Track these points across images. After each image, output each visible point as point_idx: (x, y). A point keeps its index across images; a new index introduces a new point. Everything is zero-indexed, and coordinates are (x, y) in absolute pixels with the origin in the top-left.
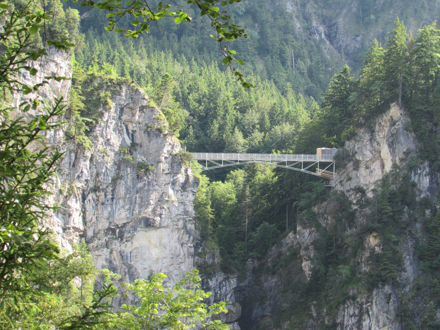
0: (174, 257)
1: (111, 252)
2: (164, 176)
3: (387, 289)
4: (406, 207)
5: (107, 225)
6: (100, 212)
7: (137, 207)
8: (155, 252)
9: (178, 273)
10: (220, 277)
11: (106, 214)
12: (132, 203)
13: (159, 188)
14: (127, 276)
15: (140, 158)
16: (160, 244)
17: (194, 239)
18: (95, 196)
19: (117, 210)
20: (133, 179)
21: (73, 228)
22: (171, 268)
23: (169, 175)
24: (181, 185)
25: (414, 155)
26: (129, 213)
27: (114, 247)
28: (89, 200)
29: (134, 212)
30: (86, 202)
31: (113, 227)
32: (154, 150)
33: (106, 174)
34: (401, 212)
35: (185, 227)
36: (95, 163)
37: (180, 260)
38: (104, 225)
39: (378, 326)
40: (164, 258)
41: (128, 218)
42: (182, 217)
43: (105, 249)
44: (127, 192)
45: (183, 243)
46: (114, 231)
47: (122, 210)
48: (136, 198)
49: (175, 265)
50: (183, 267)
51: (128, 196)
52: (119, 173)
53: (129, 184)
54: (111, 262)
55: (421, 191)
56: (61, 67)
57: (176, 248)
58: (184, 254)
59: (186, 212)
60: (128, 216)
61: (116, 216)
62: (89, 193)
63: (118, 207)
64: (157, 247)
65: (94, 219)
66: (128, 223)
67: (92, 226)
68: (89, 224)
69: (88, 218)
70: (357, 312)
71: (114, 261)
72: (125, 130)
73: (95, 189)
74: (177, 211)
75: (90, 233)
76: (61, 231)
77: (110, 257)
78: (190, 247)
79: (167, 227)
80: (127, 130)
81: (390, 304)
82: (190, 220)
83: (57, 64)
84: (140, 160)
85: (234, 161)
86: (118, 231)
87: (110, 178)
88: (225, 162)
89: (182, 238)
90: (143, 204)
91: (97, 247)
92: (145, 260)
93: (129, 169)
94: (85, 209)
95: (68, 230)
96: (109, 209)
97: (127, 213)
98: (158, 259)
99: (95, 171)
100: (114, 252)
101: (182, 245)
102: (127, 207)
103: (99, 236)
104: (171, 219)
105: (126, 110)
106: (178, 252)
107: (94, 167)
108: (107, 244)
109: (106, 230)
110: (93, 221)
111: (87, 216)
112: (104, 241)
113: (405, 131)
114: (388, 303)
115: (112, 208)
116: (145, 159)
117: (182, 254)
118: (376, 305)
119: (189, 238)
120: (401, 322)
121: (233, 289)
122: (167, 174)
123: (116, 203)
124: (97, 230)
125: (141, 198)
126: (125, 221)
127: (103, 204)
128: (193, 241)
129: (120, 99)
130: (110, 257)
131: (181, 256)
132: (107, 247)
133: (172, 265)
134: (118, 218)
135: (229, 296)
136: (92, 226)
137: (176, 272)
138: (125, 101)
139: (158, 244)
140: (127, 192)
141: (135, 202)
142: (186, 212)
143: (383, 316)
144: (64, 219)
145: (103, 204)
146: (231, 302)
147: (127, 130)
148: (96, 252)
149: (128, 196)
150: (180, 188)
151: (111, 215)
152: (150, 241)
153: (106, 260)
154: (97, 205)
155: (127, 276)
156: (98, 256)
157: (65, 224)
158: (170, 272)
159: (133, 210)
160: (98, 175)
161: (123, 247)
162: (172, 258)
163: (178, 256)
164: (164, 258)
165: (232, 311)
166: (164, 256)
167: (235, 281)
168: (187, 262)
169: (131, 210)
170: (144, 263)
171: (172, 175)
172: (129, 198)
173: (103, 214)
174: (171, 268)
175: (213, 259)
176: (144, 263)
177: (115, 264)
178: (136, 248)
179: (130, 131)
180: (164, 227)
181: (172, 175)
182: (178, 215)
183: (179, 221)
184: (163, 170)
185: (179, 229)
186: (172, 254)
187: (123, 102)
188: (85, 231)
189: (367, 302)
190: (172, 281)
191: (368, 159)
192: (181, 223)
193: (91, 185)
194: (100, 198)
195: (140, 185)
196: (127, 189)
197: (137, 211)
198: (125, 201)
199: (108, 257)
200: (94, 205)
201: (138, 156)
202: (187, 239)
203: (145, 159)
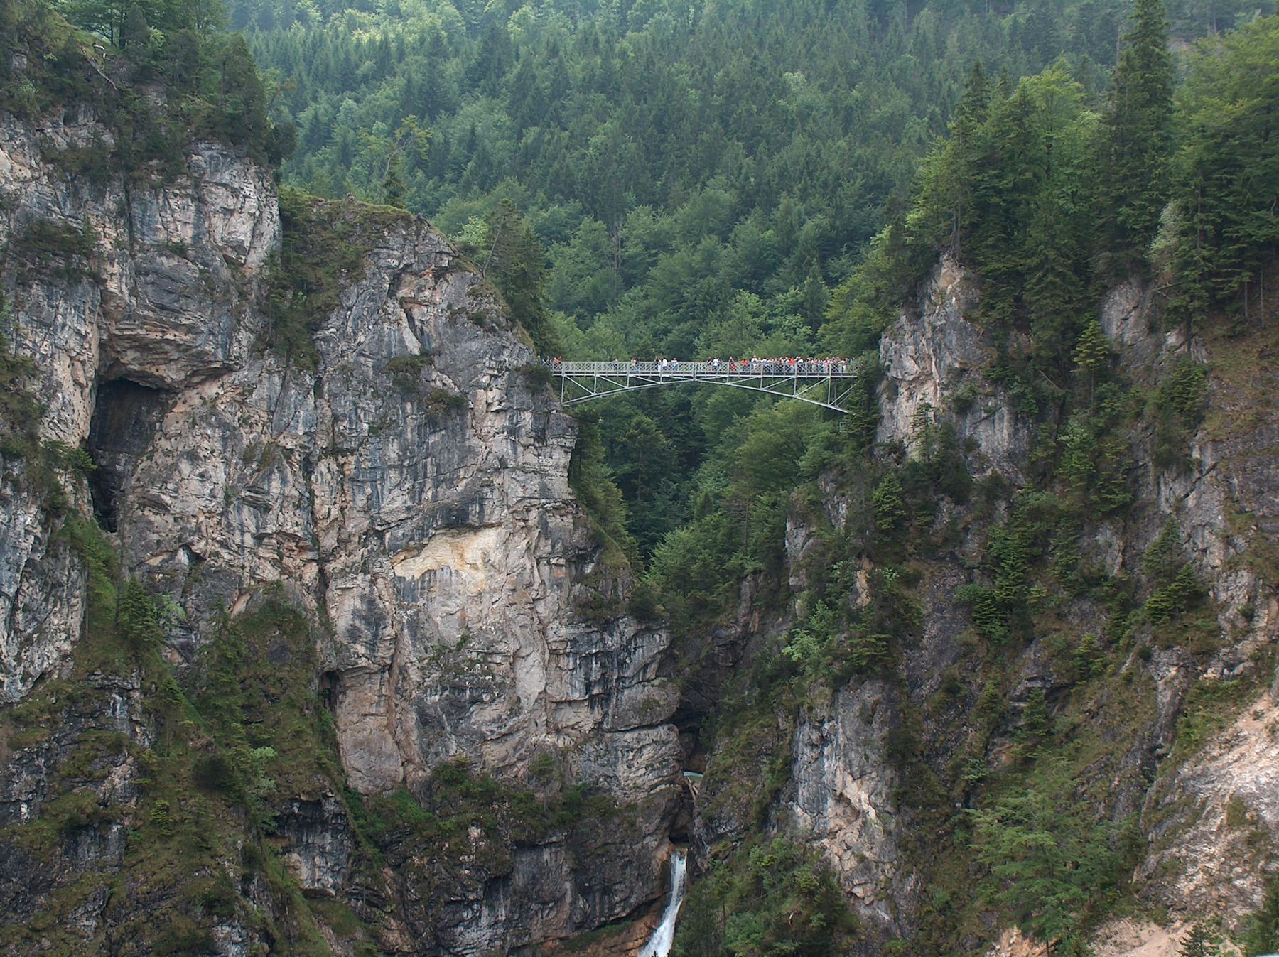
0: (519, 588)
1: (373, 582)
2: (491, 415)
3: (870, 694)
4: (948, 499)
5: (366, 524)
6: (348, 498)
7: (428, 486)
8: (476, 579)
9: (527, 621)
10: (628, 627)
11: (361, 501)
12: (415, 472)
13: (481, 443)
14: (406, 631)
15: (439, 380)
16: (486, 561)
17: (566, 548)
18: (334, 467)
19: (385, 492)
20: (420, 426)
21: (279, 533)
22: (510, 613)
23: (503, 415)
24: (533, 434)
25: (975, 375)
26: (412, 498)
27: (377, 570)
28: (322, 474)
29: (424, 496)
30: (313, 478)
31: (379, 528)
32: (465, 363)
33: (354, 418)
34: (931, 509)
35: (543, 524)
36: (327, 397)
37: (534, 594)
38: (357, 524)
39: (851, 774)
40: (495, 591)
41: (408, 509)
42: (536, 502)
43: (360, 576)
44: (405, 454)
45: (541, 558)
46: (380, 535)
47: (396, 492)
48: (425, 466)
49: (519, 606)
50: (541, 608)
51: (406, 463)
52: (385, 416)
53: (409, 436)
54: (371, 602)
55: (984, 461)
56: (245, 197)
57: (524, 569)
58: (543, 582)
59: (545, 491)
60: (409, 504)
61: (385, 507)
62: (320, 459)
63: (388, 485)
64: (477, 569)
65: (335, 512)
66: (411, 518)
67: (331, 525)
68: (323, 524)
69: (321, 511)
70: (815, 736)
71: (378, 601)
72: (405, 323)
73: (334, 451)
74: (520, 490)
75: (329, 542)
76: (249, 540)
77: (371, 591)
78: (556, 565)
79: (499, 525)
80: (411, 319)
81: (875, 725)
82: (556, 509)
83: (235, 192)
84: (438, 383)
85: (653, 378)
86: (388, 535)
87: (366, 426)
88: (634, 381)
89: (536, 547)
90: (442, 477)
91: (343, 570)
92: (450, 597)
93: (409, 406)
94: (311, 492)
95: (266, 540)
96: (369, 491)
97: (406, 497)
98: (480, 593)
99: (329, 413)
100: (380, 581)
101: (538, 564)
102: (407, 485)
103: (350, 547)
104: (509, 507)
105: (407, 278)
106: (527, 577)
107: (326, 405)
108: (364, 564)
109: (365, 534)
110: (332, 518)
111: (317, 507)
112: (358, 558)
113: (962, 320)
114: (870, 723)
115: (374, 488)
116: (449, 381)
117: (538, 580)
118: (843, 727)
119: (553, 547)
120: (900, 768)
121: (660, 653)
122: (497, 412)
123: (382, 478)
124: (344, 536)
125: (438, 466)
126: (403, 516)
127: (353, 480)
128: (564, 553)
129: (389, 256)
130: (371, 591)
131: (536, 586)
132: (365, 572)
133: (512, 604)
134: (386, 510)
135: (654, 666)
136: (331, 525)
137: (523, 620)
138: (400, 259)
139: (479, 562)
140: (405, 454)
141: (425, 476)
142: (545, 491)
143: (857, 752)
144: (256, 517)
145: (353, 480)
146: (656, 682)
147: (411, 319)
148: (339, 582)
149: (406, 463)
150: (532, 441)
151: (373, 502)
152: (461, 556)
153: (362, 597)
154: (341, 483)
155: (406, 631)
156: (343, 589)
157: (257, 528)
158: (508, 621)
159: (422, 491)
160: (336, 419)
161: (399, 571)
162: (513, 590)
163: (530, 584)
164: (495, 591)
165: (657, 702)
166: (495, 585)
167: (664, 636)
168: (549, 599)
169: (416, 494)
170: (449, 603)
171: (509, 414)
172: (409, 466)
173: (354, 501)
174: (510, 613)
175: (615, 588)
176: (449, 603)
177: (381, 606)
178: (429, 571)
179: (417, 323)
180: (491, 526)
181: (509, 414)
182: (523, 498)
183: (528, 511)
184: (489, 405)
185: (528, 529)
186: (512, 583)
187: (396, 263)
188: (315, 539)
189: (831, 718)
190: (511, 640)
191: (911, 378)
192: (533, 516)
193: (323, 442)
194: (346, 467)
195: (434, 438)
196: (404, 449)
197: (430, 494)
198: (401, 473)
199: (367, 591)
200: (333, 483)
201: (434, 375)
202: (549, 549)
203: (449, 381)
